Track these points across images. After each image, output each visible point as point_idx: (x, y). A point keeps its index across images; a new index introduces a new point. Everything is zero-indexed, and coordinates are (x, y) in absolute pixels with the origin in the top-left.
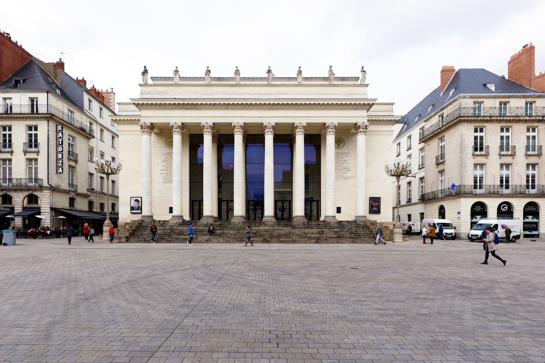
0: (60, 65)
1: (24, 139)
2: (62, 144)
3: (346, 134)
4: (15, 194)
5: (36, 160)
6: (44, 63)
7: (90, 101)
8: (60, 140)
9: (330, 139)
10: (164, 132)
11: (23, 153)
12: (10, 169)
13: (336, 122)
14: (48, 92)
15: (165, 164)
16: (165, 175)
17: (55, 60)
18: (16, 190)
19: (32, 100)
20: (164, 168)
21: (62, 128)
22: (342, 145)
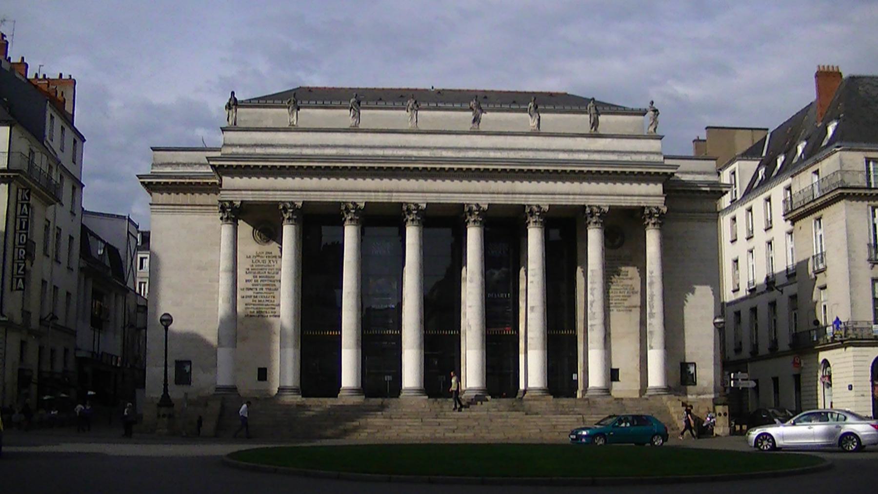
16: (250, 301)
20: (249, 285)
22: (617, 242)
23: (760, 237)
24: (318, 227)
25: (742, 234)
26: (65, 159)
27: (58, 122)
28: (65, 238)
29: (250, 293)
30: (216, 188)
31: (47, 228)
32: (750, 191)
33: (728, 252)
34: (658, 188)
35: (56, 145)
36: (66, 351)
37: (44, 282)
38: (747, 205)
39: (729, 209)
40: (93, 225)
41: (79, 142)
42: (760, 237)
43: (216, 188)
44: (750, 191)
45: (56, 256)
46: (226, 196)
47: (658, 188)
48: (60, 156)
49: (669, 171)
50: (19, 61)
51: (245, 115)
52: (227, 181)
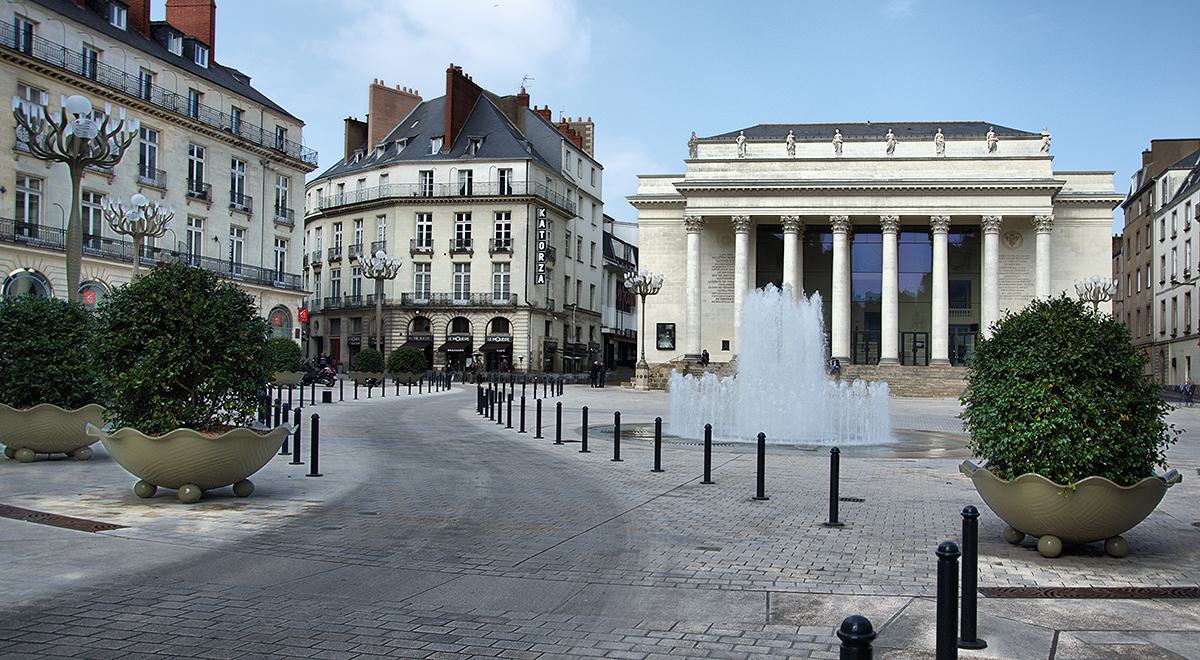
0: (524, 98)
1: (491, 233)
2: (544, 238)
3: (1017, 230)
4: (475, 316)
5: (508, 264)
6: (496, 96)
7: (568, 152)
8: (542, 232)
9: (991, 241)
10: (718, 230)
11: (489, 255)
12: (468, 278)
13: (999, 214)
14: (528, 161)
15: (716, 272)
17: (516, 92)
18: (476, 312)
19: (502, 172)
20: (715, 278)
21: (545, 213)
22: (1018, 243)
23: (1182, 236)
24: (766, 235)
25: (1168, 234)
26: (584, 183)
27: (574, 155)
28: (586, 246)
29: (716, 285)
30: (682, 206)
31: (568, 236)
32: (1178, 197)
33: (1159, 249)
34: (1047, 200)
35: (573, 173)
36: (592, 328)
37: (567, 278)
38: (1174, 209)
39: (1161, 213)
40: (619, 232)
41: (596, 169)
42: (1182, 236)
43: (682, 206)
44: (1178, 197)
45: (579, 257)
46: (689, 213)
47: (1047, 200)
48: (579, 183)
49: (1056, 186)
50: (543, 108)
51: (704, 151)
52: (691, 202)
